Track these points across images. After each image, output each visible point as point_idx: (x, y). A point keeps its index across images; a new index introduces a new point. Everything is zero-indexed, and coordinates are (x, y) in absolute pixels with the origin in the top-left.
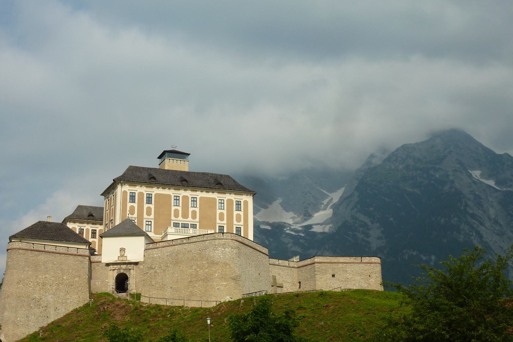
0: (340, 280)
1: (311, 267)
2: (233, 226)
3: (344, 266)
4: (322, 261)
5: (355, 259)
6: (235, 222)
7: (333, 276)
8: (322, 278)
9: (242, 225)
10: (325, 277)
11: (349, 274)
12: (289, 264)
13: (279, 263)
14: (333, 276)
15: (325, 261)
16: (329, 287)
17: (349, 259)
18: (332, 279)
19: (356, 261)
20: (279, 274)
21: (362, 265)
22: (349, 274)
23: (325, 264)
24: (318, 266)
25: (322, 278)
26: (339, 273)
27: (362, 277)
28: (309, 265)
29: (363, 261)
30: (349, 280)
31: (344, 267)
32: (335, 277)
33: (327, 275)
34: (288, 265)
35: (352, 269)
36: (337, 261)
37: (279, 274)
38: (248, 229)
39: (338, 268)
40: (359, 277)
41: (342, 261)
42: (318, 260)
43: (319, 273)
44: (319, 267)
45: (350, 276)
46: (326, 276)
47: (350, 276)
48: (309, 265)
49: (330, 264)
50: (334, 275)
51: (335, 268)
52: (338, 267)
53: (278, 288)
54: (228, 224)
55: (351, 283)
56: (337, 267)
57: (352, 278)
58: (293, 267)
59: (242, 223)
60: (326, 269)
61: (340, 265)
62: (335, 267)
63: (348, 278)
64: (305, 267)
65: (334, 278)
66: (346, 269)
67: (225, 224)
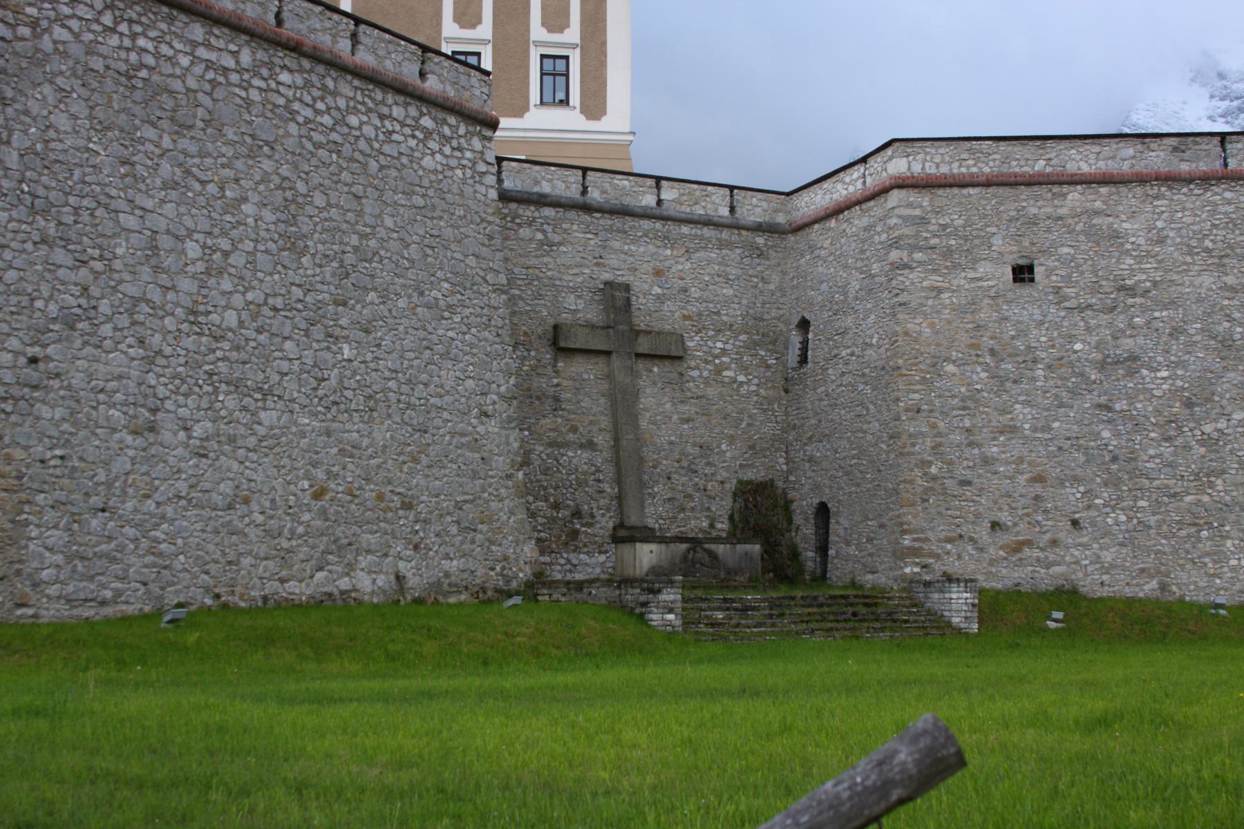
0: (1072, 303)
1: (865, 221)
2: (527, 51)
3: (1098, 204)
4: (944, 169)
5: (1175, 149)
6: (537, 31)
7: (1023, 273)
8: (940, 291)
9: (574, 46)
10: (960, 280)
11: (1139, 259)
12: (732, 209)
13: (660, 202)
14: (1023, 273)
15: (963, 170)
16: (992, 352)
17: (1131, 152)
18: (1010, 295)
19: (1184, 167)
20: (658, 273)
21: (1228, 195)
22: (1139, 259)
23: (965, 191)
24: (910, 205)
25: (940, 291)
26: (1065, 250)
27: (1230, 280)
28: (859, 202)
29: (1232, 164)
30: (1138, 300)
31: (1097, 213)
32: (1032, 280)
33: (975, 270)
34: (725, 211)
35: (1160, 224)
36: (1048, 170)
37: (658, 273)
38: (602, 64)
39: (1060, 218)
40: (1207, 280)
41: (1085, 168)
42: (917, 168)
43: (918, 256)
44: (918, 212)
45: (1143, 271)
46: (971, 275)
47: (1143, 271)
48: (859, 202)
49: (1001, 190)
50: (1030, 269)
51: (1033, 222)
52: (1063, 211)
53: (641, 365)
54: (498, 43)
55: (1148, 323)
56: (1049, 210)
57: (1155, 284)
58: (758, 228)
59: (573, 34)
60: (968, 223)
61: (1074, 197)
62: (1033, 210)
63: (1132, 288)
64: (832, 223)
65: (1024, 290)
66: (1110, 226)
67: (484, 42)
